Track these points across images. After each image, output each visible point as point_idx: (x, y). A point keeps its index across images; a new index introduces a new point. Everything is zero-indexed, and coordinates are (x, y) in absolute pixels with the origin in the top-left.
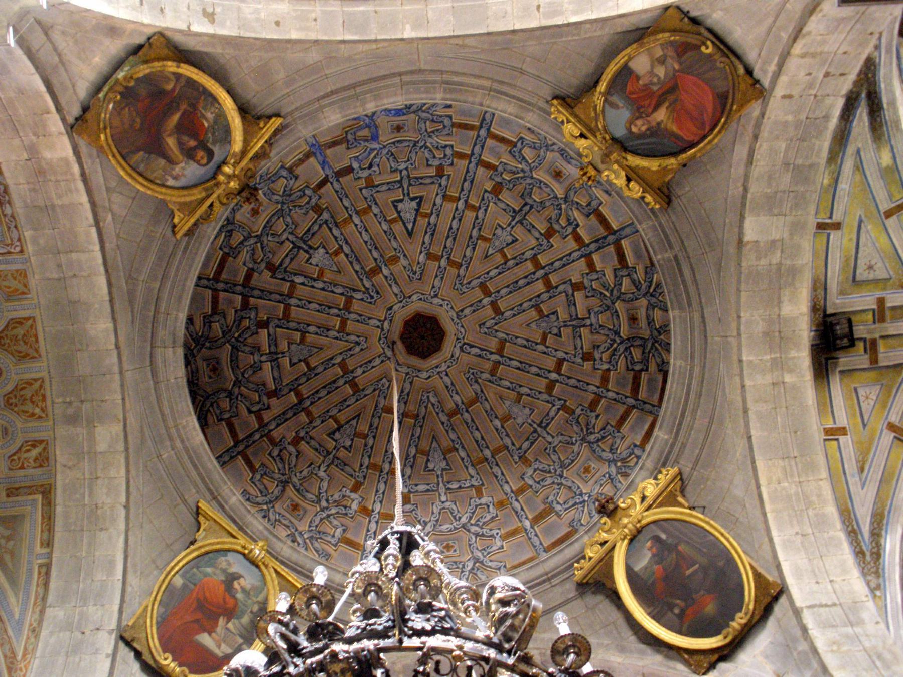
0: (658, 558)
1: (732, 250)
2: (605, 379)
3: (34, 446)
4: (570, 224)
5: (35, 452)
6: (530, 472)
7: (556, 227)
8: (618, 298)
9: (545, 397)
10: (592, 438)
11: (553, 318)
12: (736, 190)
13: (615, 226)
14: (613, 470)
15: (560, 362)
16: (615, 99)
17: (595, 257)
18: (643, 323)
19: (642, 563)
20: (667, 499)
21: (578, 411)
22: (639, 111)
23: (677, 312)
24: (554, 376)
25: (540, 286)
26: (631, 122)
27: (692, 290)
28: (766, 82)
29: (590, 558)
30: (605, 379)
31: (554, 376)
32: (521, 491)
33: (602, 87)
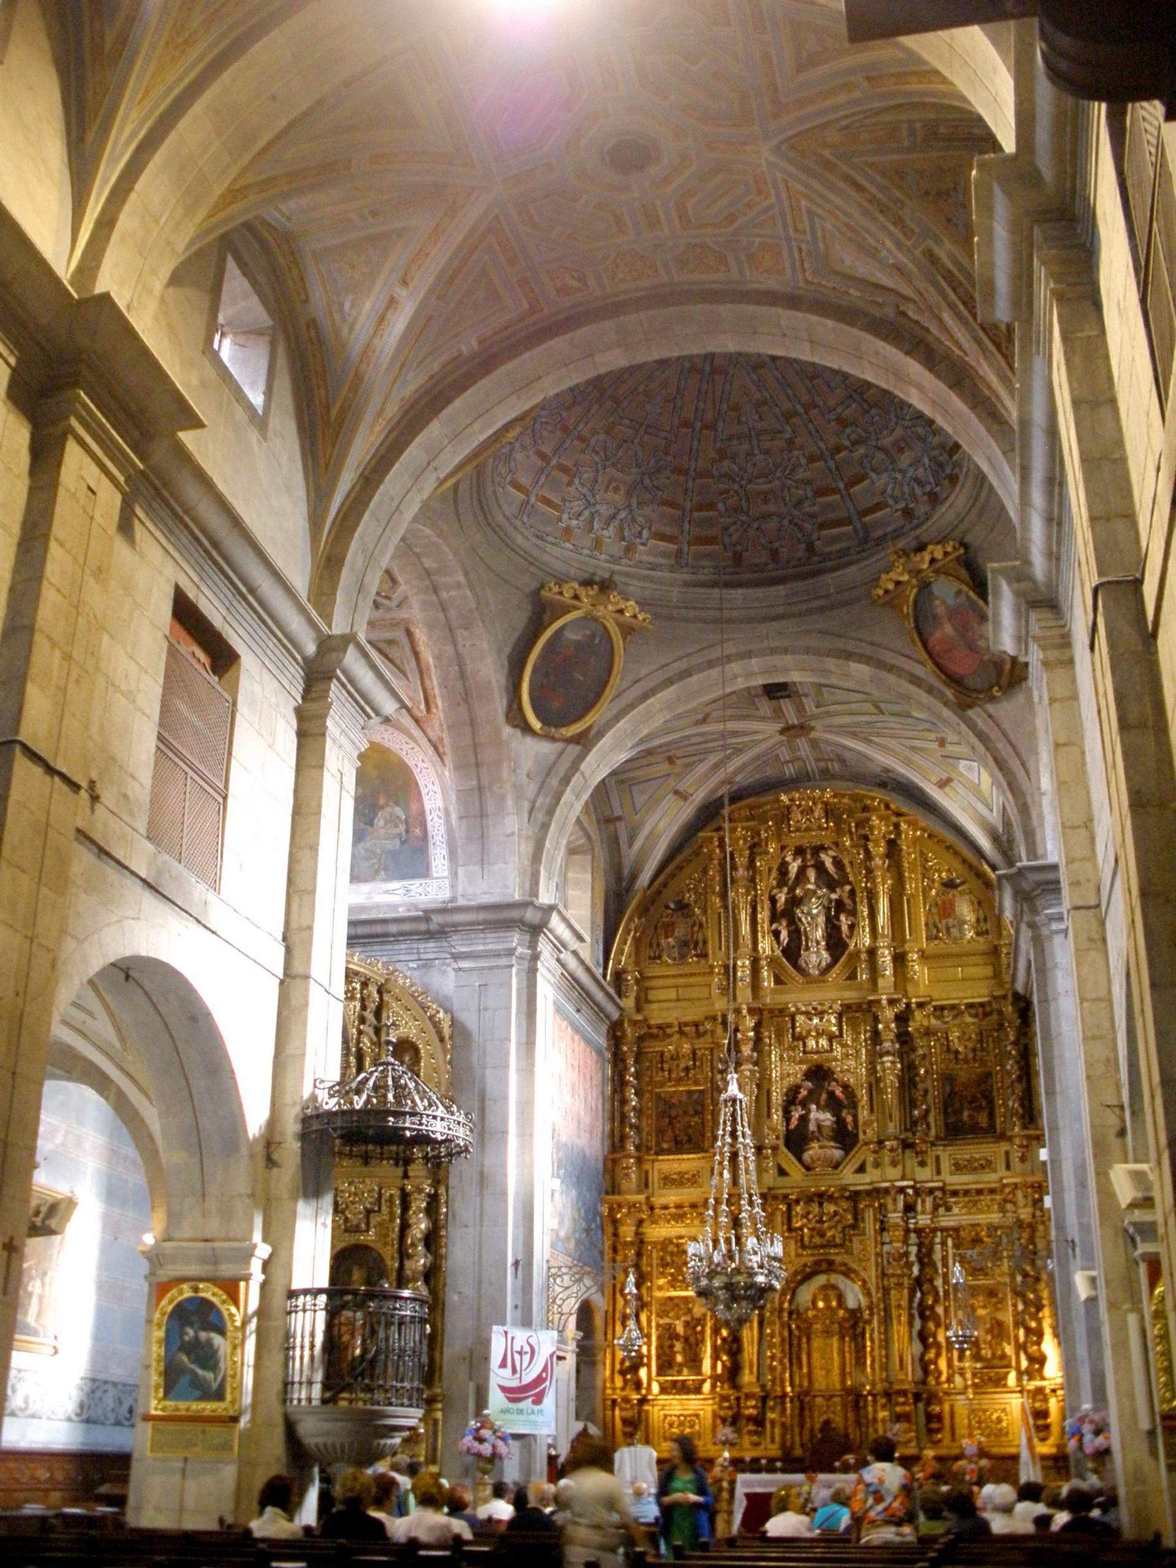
0: (578, 644)
1: (840, 644)
2: (706, 474)
3: (579, 280)
4: (854, 444)
5: (575, 284)
6: (602, 437)
7: (848, 431)
8: (783, 485)
9: (676, 422)
10: (647, 481)
11: (756, 417)
12: (890, 658)
13: (856, 489)
14: (623, 514)
15: (712, 426)
16: (963, 598)
17: (820, 464)
18: (765, 508)
19: (572, 636)
20: (627, 630)
21: (670, 458)
22: (953, 614)
23: (783, 593)
24: (698, 425)
25: (787, 405)
26: (944, 602)
27: (804, 607)
28: (970, 713)
29: (561, 593)
30: (706, 474)
31: (698, 425)
32: (581, 438)
33: (971, 594)
